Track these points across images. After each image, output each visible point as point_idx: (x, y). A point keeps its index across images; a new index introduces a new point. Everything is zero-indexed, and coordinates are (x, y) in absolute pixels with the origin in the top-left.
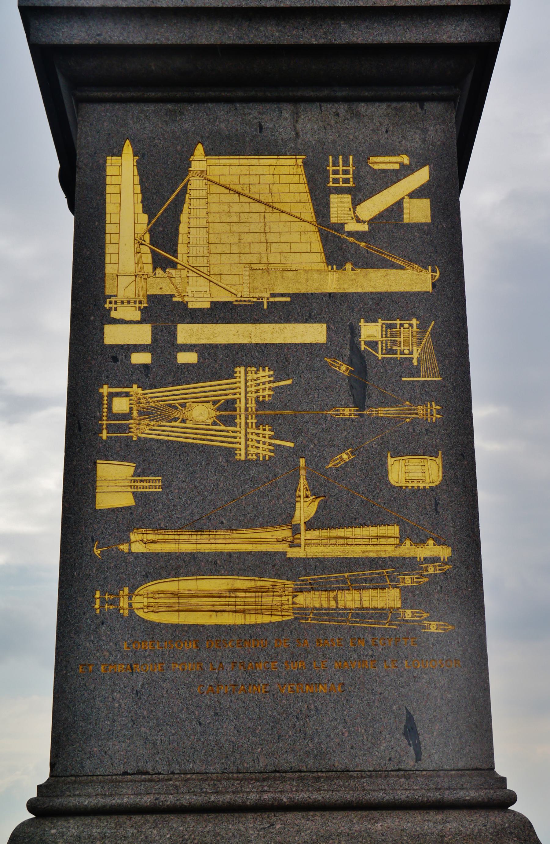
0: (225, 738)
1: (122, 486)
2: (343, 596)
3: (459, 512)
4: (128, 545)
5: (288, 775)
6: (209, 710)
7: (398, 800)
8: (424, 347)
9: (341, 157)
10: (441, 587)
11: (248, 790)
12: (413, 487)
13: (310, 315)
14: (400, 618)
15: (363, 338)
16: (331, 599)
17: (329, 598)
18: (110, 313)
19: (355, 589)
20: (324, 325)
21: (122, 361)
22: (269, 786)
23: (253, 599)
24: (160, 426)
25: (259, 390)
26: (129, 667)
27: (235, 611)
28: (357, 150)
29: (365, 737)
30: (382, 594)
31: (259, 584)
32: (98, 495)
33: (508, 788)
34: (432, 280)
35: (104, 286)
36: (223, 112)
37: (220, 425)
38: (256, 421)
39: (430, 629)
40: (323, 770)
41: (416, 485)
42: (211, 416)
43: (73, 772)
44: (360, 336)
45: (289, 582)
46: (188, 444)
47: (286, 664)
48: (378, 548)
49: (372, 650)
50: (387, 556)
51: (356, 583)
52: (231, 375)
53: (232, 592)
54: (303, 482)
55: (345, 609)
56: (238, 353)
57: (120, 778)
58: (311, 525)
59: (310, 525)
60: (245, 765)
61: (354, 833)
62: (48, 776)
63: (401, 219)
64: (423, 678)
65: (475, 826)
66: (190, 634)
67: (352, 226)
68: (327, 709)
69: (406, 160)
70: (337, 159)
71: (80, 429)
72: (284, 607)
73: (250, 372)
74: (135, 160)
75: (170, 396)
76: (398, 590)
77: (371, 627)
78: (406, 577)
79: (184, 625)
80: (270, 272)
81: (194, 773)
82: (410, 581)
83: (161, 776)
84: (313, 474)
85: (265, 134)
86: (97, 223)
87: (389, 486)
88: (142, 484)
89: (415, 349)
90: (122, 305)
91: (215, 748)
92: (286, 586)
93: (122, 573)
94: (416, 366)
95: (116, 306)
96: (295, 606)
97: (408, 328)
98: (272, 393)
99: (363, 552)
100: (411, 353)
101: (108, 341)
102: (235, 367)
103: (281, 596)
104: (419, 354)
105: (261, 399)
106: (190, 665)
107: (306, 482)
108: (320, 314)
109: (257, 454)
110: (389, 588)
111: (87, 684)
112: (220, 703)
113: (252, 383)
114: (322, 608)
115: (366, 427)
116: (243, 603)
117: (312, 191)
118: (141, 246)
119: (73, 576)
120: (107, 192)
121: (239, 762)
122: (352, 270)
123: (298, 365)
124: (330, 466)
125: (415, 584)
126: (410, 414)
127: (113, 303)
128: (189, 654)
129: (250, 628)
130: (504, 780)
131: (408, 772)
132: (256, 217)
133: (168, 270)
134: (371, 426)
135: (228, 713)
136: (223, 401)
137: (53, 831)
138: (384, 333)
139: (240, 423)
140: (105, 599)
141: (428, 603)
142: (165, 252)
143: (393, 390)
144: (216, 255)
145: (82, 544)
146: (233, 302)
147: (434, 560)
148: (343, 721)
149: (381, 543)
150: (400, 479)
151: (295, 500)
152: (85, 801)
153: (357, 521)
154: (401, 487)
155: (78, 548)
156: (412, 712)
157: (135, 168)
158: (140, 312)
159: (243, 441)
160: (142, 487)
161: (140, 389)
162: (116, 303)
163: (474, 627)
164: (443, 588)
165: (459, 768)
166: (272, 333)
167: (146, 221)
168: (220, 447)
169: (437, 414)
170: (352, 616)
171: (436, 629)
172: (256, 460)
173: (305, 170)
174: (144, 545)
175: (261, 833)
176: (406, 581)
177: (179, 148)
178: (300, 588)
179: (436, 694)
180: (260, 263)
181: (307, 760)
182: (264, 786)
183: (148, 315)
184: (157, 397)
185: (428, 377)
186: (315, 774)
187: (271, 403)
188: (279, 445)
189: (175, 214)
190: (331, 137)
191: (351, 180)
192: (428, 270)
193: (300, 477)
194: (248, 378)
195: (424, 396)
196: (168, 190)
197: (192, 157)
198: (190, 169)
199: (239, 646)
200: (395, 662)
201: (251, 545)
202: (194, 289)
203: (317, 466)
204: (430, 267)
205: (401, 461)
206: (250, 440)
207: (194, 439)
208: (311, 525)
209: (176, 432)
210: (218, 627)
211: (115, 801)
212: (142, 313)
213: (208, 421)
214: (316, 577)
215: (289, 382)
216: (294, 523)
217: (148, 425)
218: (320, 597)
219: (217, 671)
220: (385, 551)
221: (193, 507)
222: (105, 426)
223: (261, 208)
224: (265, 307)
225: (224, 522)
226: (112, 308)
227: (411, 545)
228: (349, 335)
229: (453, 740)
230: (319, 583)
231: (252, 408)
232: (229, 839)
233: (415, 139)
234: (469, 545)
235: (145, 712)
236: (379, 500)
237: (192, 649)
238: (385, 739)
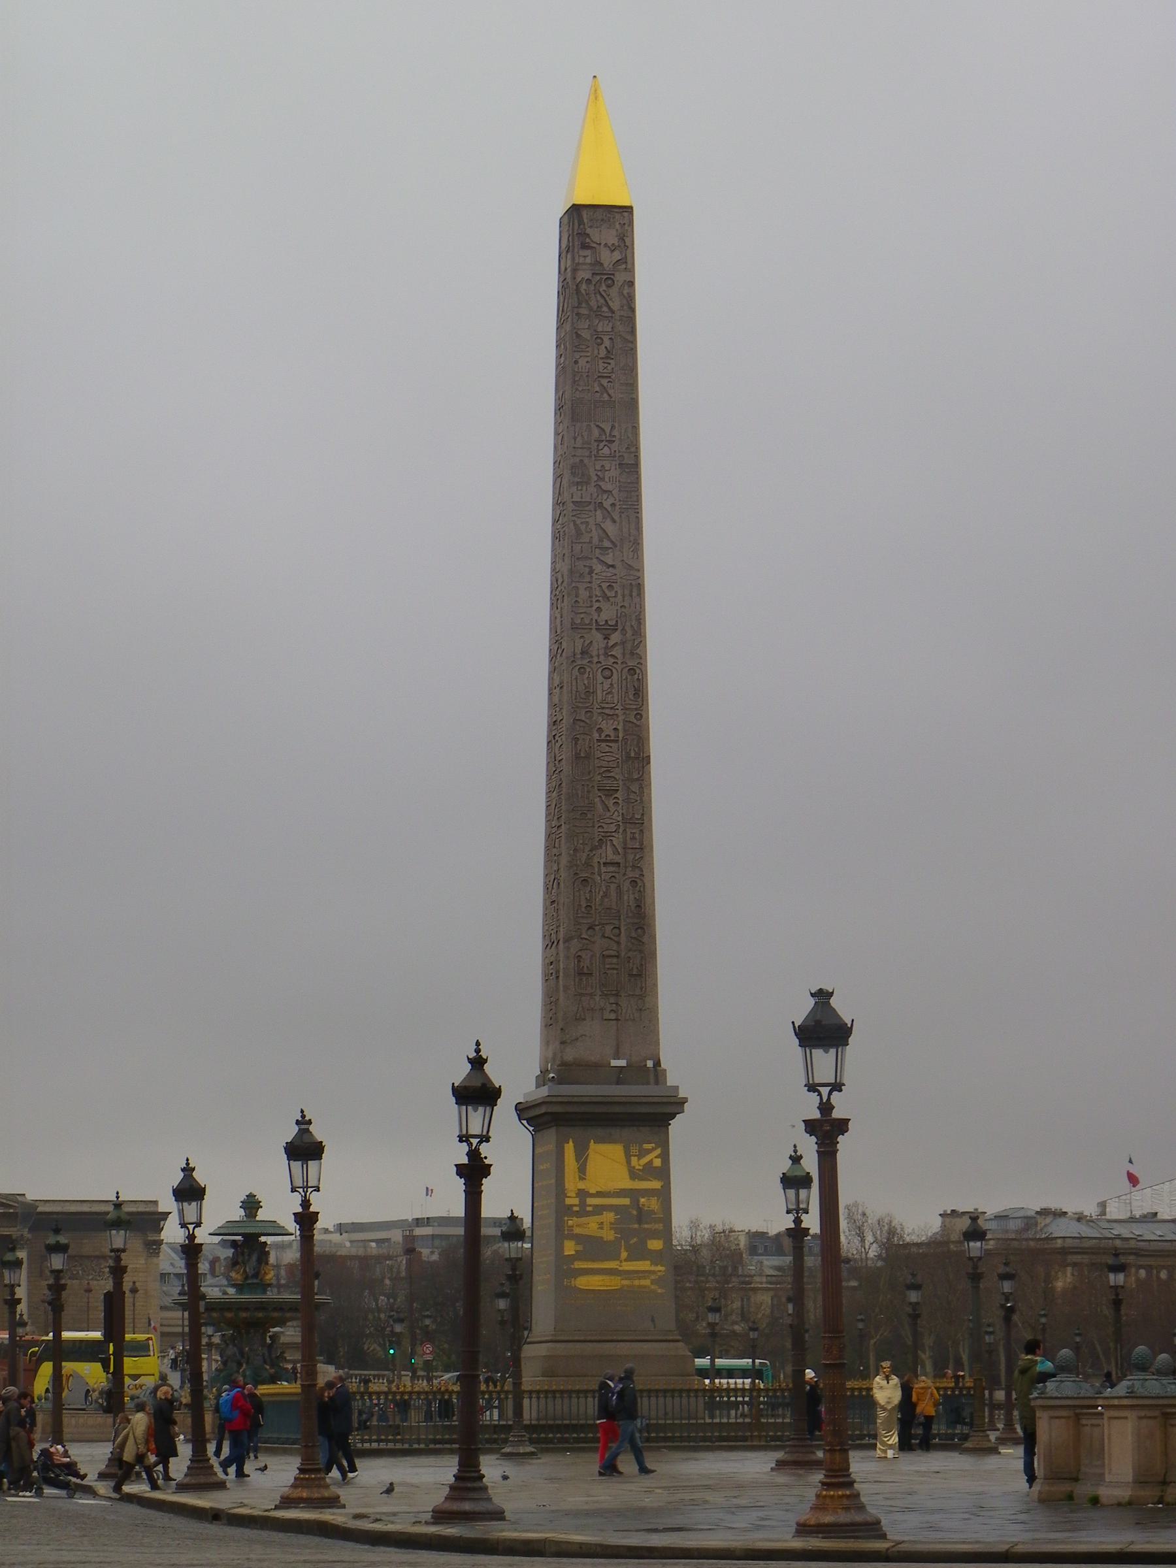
15: (641, 1203)
54: (623, 1247)
58: (626, 1260)
67: (637, 1167)
147: (660, 1271)
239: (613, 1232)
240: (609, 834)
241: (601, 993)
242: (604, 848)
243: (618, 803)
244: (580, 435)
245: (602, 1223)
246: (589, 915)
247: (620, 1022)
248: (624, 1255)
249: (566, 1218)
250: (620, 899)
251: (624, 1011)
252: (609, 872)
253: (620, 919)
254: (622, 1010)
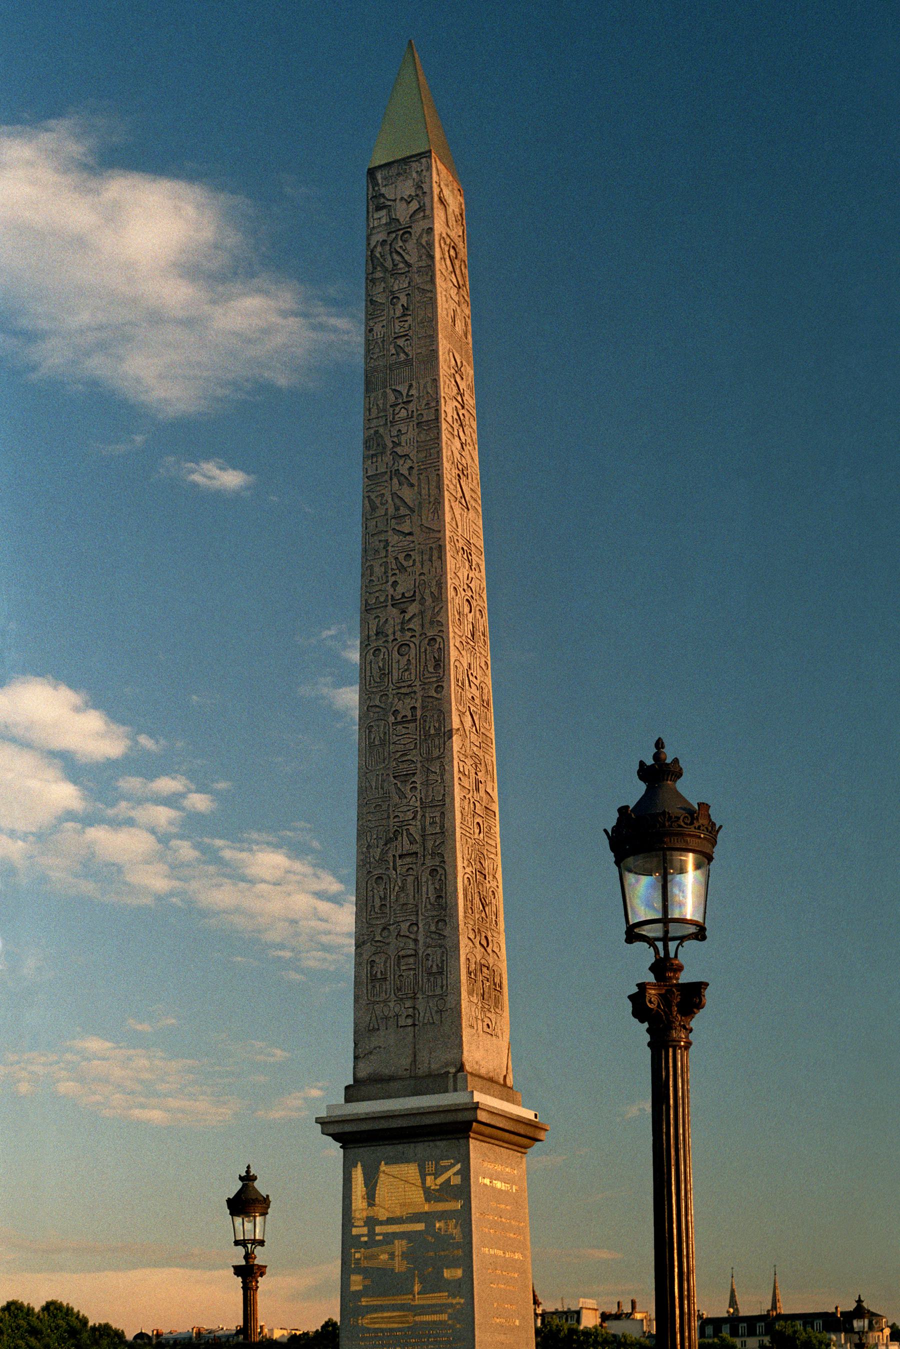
54: (417, 1279)
101: (353, 1233)
223: (403, 1182)
239: (405, 1263)
240: (405, 823)
241: (396, 999)
242: (400, 839)
243: (415, 787)
244: (375, 405)
246: (383, 915)
247: (417, 1028)
248: (417, 1288)
250: (418, 891)
251: (422, 1015)
252: (405, 865)
253: (417, 914)
254: (419, 1013)
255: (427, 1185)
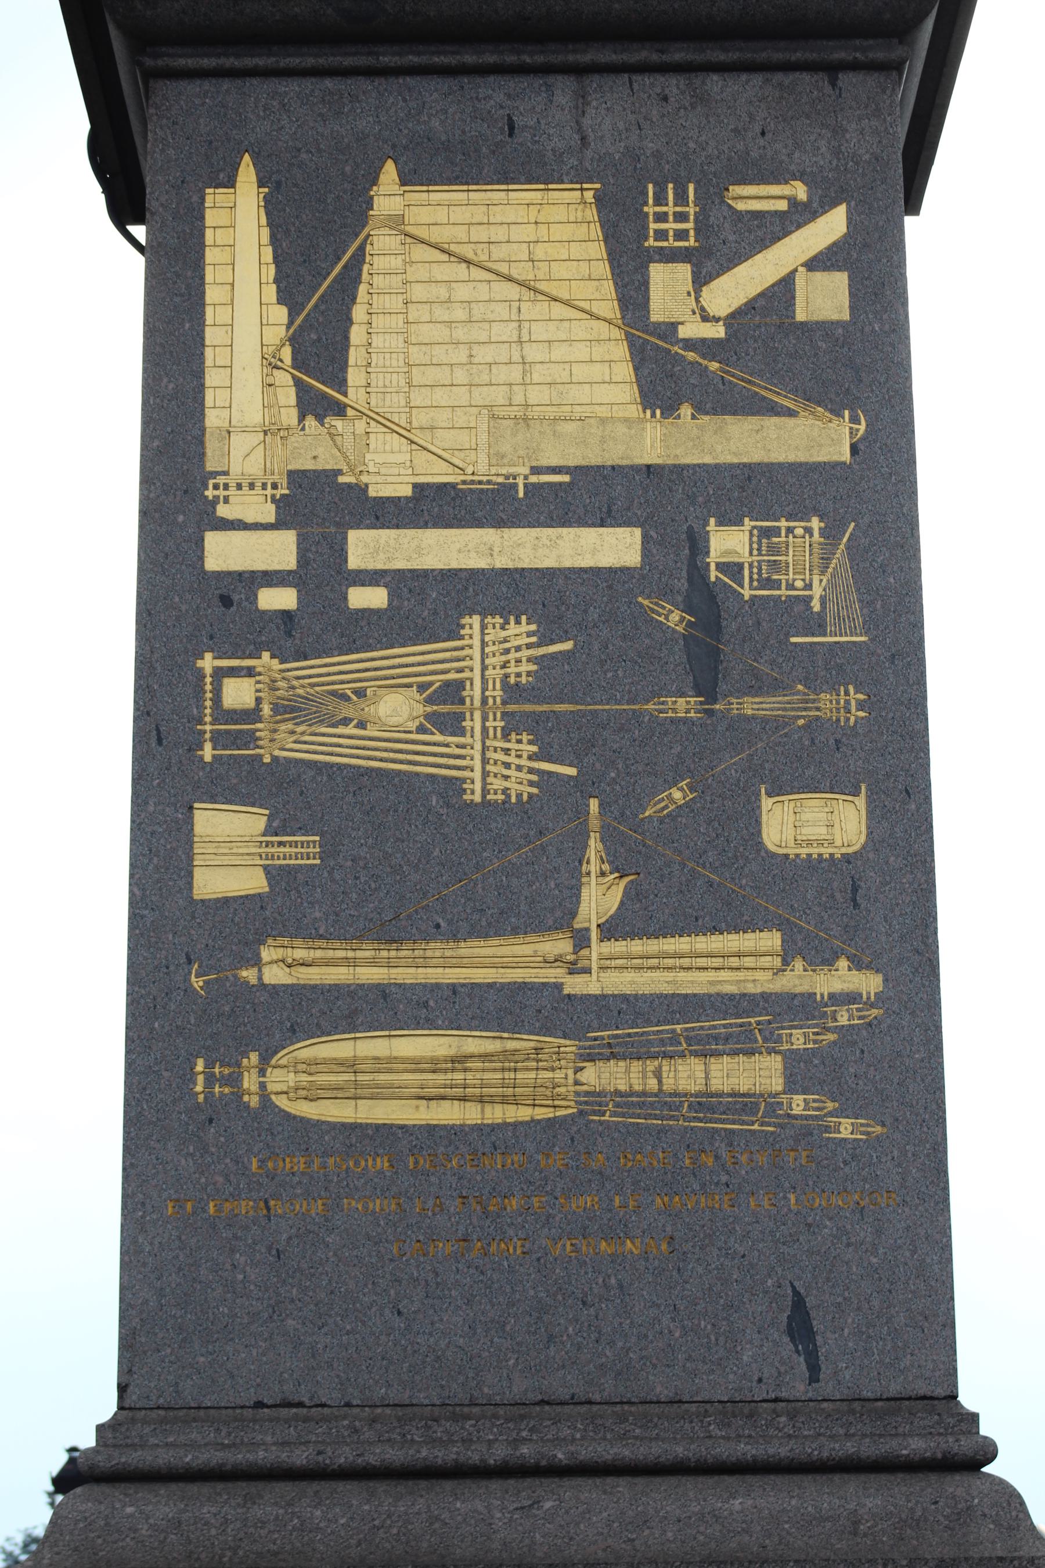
0: (447, 1340)
1: (242, 854)
2: (673, 1069)
3: (897, 904)
4: (256, 969)
5: (567, 1409)
6: (415, 1287)
7: (773, 1456)
8: (833, 576)
9: (671, 186)
10: (862, 1052)
11: (491, 1437)
12: (809, 855)
13: (609, 511)
14: (781, 1112)
15: (714, 557)
16: (650, 1074)
17: (644, 1072)
18: (215, 508)
19: (696, 1054)
20: (638, 532)
21: (239, 604)
22: (532, 1430)
23: (499, 1075)
24: (316, 734)
25: (509, 662)
26: (262, 1204)
27: (463, 1099)
28: (702, 171)
29: (713, 1338)
30: (747, 1066)
31: (511, 1045)
32: (198, 873)
33: (983, 1432)
34: (851, 437)
35: (204, 454)
36: (435, 95)
37: (433, 733)
38: (502, 724)
39: (840, 1132)
40: (633, 1400)
41: (816, 851)
42: (415, 714)
43: (161, 1401)
44: (708, 553)
45: (568, 1042)
46: (370, 770)
47: (562, 1201)
48: (741, 975)
49: (728, 1174)
50: (759, 990)
51: (698, 1044)
52: (454, 634)
53: (459, 1061)
54: (594, 846)
55: (675, 1094)
56: (466, 589)
57: (248, 1413)
58: (610, 930)
59: (609, 930)
60: (486, 1390)
61: (690, 1517)
62: (114, 1408)
63: (789, 314)
64: (826, 1227)
65: (917, 1502)
66: (377, 1143)
67: (692, 329)
68: (641, 1286)
69: (800, 191)
70: (664, 190)
71: (160, 741)
72: (558, 1089)
73: (490, 626)
74: (261, 196)
75: (334, 674)
76: (779, 1058)
77: (726, 1130)
78: (794, 1031)
79: (367, 1124)
80: (531, 423)
81: (388, 1405)
82: (802, 1040)
83: (326, 1411)
84: (615, 828)
85: (521, 140)
86: (187, 325)
87: (763, 853)
88: (282, 849)
89: (816, 579)
90: (239, 492)
91: (428, 1359)
92: (562, 1049)
93: (245, 1026)
94: (818, 614)
95: (226, 493)
96: (578, 1088)
97: (804, 537)
98: (534, 668)
99: (711, 983)
100: (809, 586)
101: (212, 564)
102: (461, 616)
103: (553, 1069)
104: (824, 590)
105: (512, 680)
106: (378, 1202)
107: (600, 846)
108: (628, 509)
109: (505, 791)
110: (761, 1053)
111: (183, 1237)
112: (437, 1275)
113: (495, 648)
114: (631, 1093)
115: (718, 736)
116: (479, 1082)
117: (614, 258)
118: (276, 372)
119: (153, 1029)
120: (207, 262)
121: (474, 1384)
122: (693, 417)
123: (585, 611)
124: (647, 814)
125: (811, 1046)
126: (805, 709)
127: (221, 487)
128: (376, 1180)
129: (493, 1130)
130: (974, 1418)
131: (793, 1404)
132: (501, 311)
133: (327, 420)
134: (728, 733)
135: (453, 1292)
136: (437, 684)
137: (129, 1510)
138: (755, 546)
139: (472, 728)
140: (213, 1074)
141: (837, 1082)
142: (323, 383)
143: (772, 663)
144: (423, 389)
145: (167, 968)
146: (457, 484)
147: (850, 998)
148: (672, 1308)
149: (746, 965)
150: (784, 839)
151: (579, 880)
152: (186, 1456)
153: (700, 922)
154: (787, 856)
155: (161, 975)
156: (802, 1291)
157: (262, 211)
158: (274, 506)
159: (477, 764)
160: (281, 855)
161: (276, 661)
162: (226, 487)
163: (925, 1129)
164: (866, 1052)
165: (891, 1395)
166: (535, 548)
167: (285, 320)
168: (432, 776)
169: (858, 710)
170: (689, 1106)
171: (852, 1133)
172: (504, 802)
173: (599, 212)
174: (287, 970)
175: (516, 1516)
176: (794, 1040)
177: (348, 169)
178: (589, 1054)
179: (849, 1256)
180: (511, 405)
181: (602, 1381)
182: (520, 1430)
183: (290, 510)
184: (310, 677)
185: (841, 635)
186: (618, 1408)
187: (533, 688)
188: (550, 774)
189: (342, 304)
190: (651, 145)
191: (692, 233)
192: (843, 418)
193: (589, 836)
194: (487, 638)
195: (834, 672)
196: (327, 255)
197: (375, 188)
198: (371, 213)
199: (472, 1166)
200: (771, 1196)
201: (494, 970)
202: (379, 458)
203: (622, 814)
204: (847, 412)
205: (786, 803)
206: (492, 762)
207: (381, 760)
208: (610, 930)
209: (347, 747)
210: (431, 1129)
211: (239, 1457)
212: (278, 508)
213: (410, 724)
214: (620, 1032)
215: (568, 646)
216: (576, 926)
217: (293, 732)
218: (628, 1071)
219: (430, 1214)
220: (754, 981)
221: (382, 895)
222: (208, 736)
223: (512, 291)
224: (521, 494)
225: (442, 924)
226: (218, 497)
227: (805, 970)
228: (687, 551)
229: (881, 1343)
230: (626, 1043)
231: (494, 697)
232: (457, 1528)
233: (819, 148)
234: (917, 970)
235: (294, 1291)
236: (744, 882)
237: (381, 1172)
238: (750, 1342)
245: (453, 691)
249: (208, 663)
255: (658, 313)
